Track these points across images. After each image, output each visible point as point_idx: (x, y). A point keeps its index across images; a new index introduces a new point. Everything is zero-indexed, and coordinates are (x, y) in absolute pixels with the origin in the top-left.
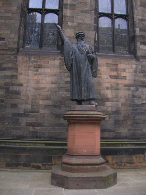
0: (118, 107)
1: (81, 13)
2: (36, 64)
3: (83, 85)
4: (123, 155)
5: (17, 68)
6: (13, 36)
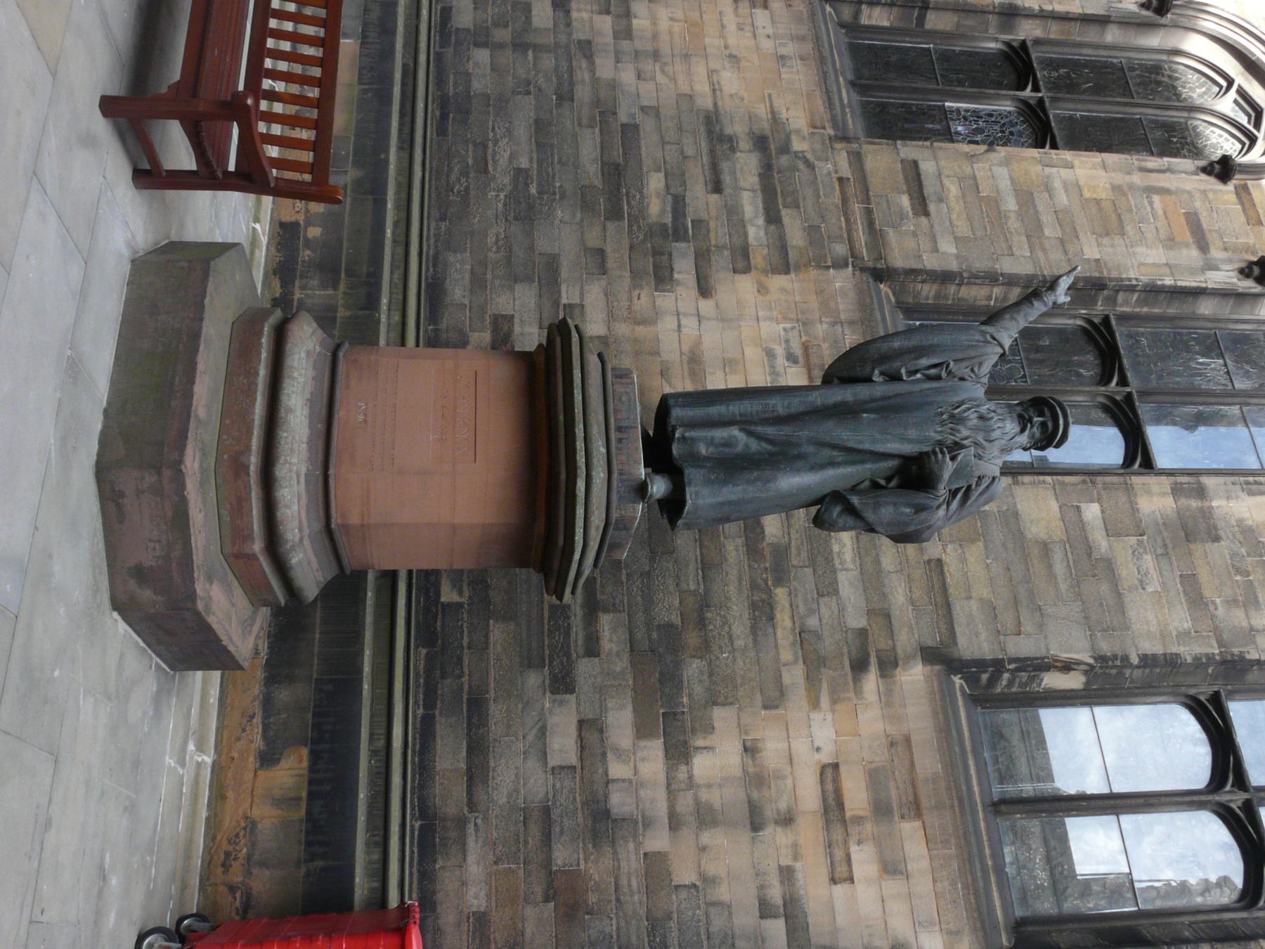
0: (636, 830)
1: (1181, 576)
3: (759, 429)
4: (303, 869)
5: (787, 272)
6: (948, 246)
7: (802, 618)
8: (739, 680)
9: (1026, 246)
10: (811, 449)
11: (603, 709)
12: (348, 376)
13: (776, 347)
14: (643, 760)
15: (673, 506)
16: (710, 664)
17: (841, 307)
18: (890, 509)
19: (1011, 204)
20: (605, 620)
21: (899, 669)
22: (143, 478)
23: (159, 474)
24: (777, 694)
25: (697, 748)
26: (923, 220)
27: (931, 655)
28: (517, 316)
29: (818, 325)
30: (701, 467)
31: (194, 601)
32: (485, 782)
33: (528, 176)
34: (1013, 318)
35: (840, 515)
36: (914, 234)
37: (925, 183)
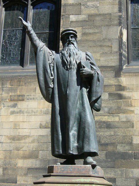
2: (13, 94)
16: (119, 143)
24: (129, 123)
29: (3, 95)
34: (36, 41)
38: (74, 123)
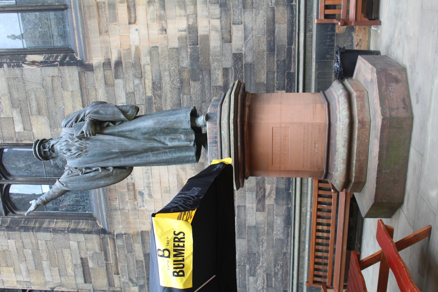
3: (160, 145)
5: (142, 232)
6: (74, 244)
7: (141, 83)
8: (167, 58)
9: (39, 245)
10: (140, 137)
11: (222, 47)
12: (322, 163)
13: (148, 199)
14: (206, 27)
15: (194, 115)
16: (179, 65)
17: (120, 217)
18: (108, 113)
19: (45, 264)
20: (220, 83)
21: (102, 62)
22: (396, 114)
23: (390, 115)
24: (152, 52)
25: (185, 31)
26: (83, 257)
27: (89, 68)
28: (255, 211)
29: (130, 208)
30: (184, 129)
31: (377, 71)
32: (268, 18)
33: (250, 273)
35: (129, 110)
36: (87, 250)
37: (82, 273)
38: (155, 140)
